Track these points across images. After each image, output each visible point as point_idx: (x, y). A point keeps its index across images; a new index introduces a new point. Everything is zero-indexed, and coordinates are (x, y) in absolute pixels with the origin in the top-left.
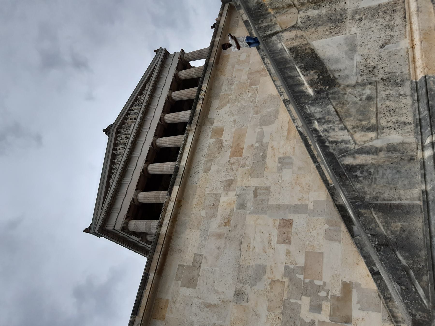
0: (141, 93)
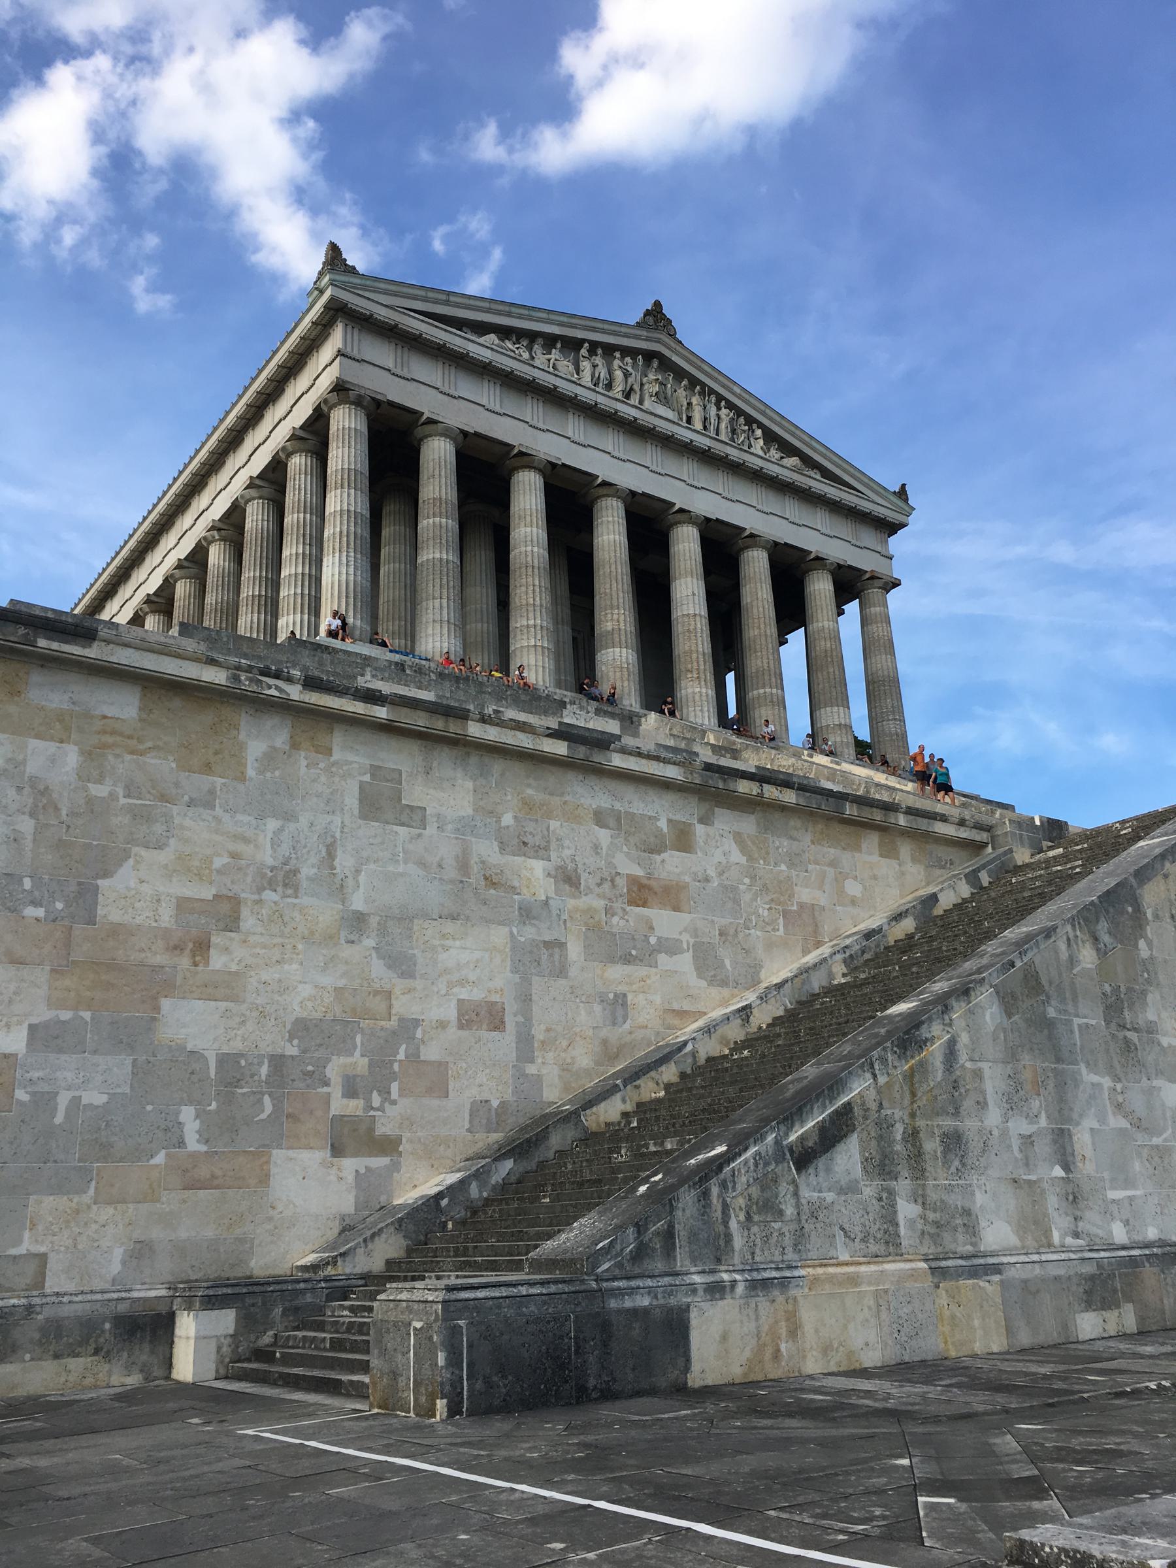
0: (771, 438)
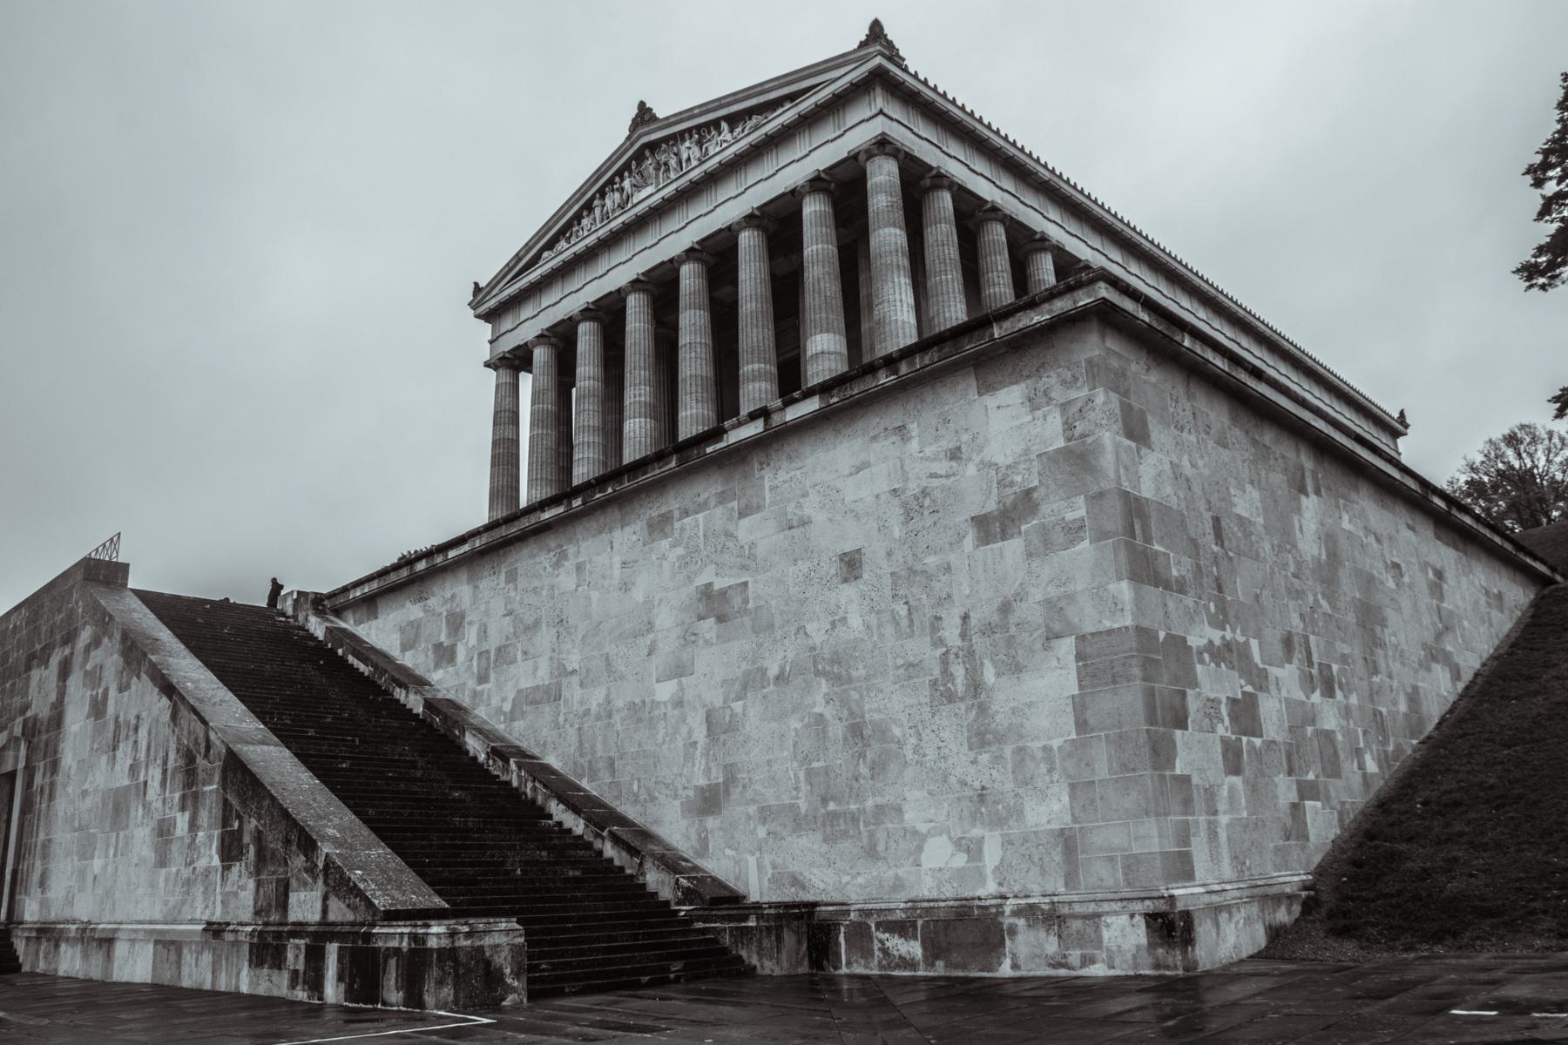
0: (734, 120)
